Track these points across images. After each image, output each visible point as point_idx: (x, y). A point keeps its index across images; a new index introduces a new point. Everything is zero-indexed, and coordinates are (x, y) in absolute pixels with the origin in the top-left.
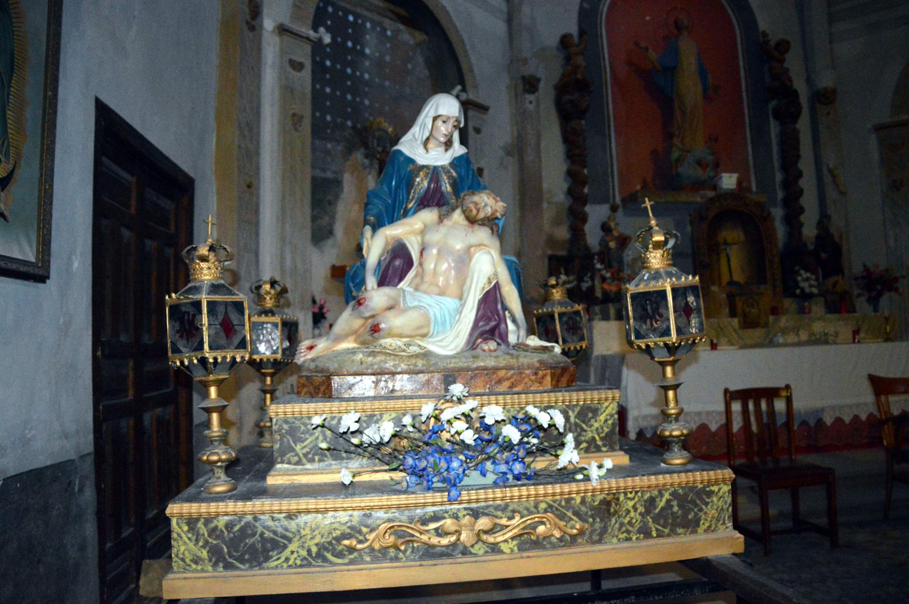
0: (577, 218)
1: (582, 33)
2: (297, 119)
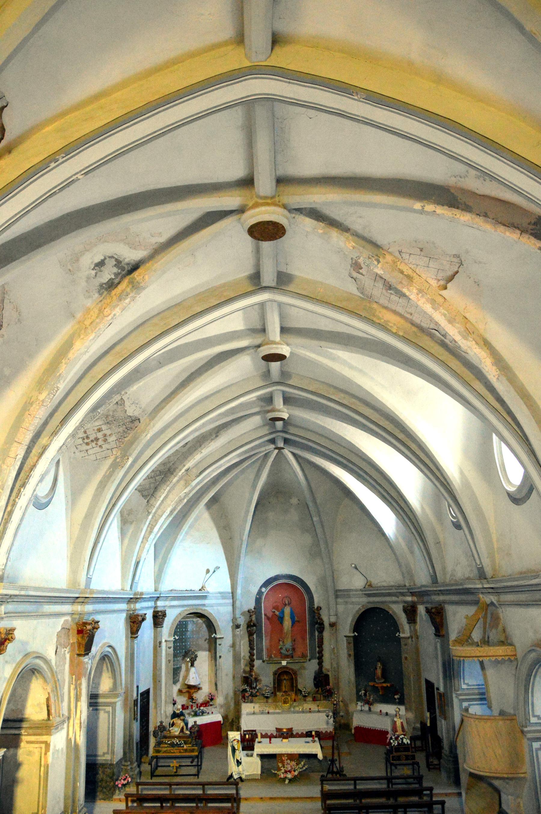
0: (252, 666)
2: (169, 661)
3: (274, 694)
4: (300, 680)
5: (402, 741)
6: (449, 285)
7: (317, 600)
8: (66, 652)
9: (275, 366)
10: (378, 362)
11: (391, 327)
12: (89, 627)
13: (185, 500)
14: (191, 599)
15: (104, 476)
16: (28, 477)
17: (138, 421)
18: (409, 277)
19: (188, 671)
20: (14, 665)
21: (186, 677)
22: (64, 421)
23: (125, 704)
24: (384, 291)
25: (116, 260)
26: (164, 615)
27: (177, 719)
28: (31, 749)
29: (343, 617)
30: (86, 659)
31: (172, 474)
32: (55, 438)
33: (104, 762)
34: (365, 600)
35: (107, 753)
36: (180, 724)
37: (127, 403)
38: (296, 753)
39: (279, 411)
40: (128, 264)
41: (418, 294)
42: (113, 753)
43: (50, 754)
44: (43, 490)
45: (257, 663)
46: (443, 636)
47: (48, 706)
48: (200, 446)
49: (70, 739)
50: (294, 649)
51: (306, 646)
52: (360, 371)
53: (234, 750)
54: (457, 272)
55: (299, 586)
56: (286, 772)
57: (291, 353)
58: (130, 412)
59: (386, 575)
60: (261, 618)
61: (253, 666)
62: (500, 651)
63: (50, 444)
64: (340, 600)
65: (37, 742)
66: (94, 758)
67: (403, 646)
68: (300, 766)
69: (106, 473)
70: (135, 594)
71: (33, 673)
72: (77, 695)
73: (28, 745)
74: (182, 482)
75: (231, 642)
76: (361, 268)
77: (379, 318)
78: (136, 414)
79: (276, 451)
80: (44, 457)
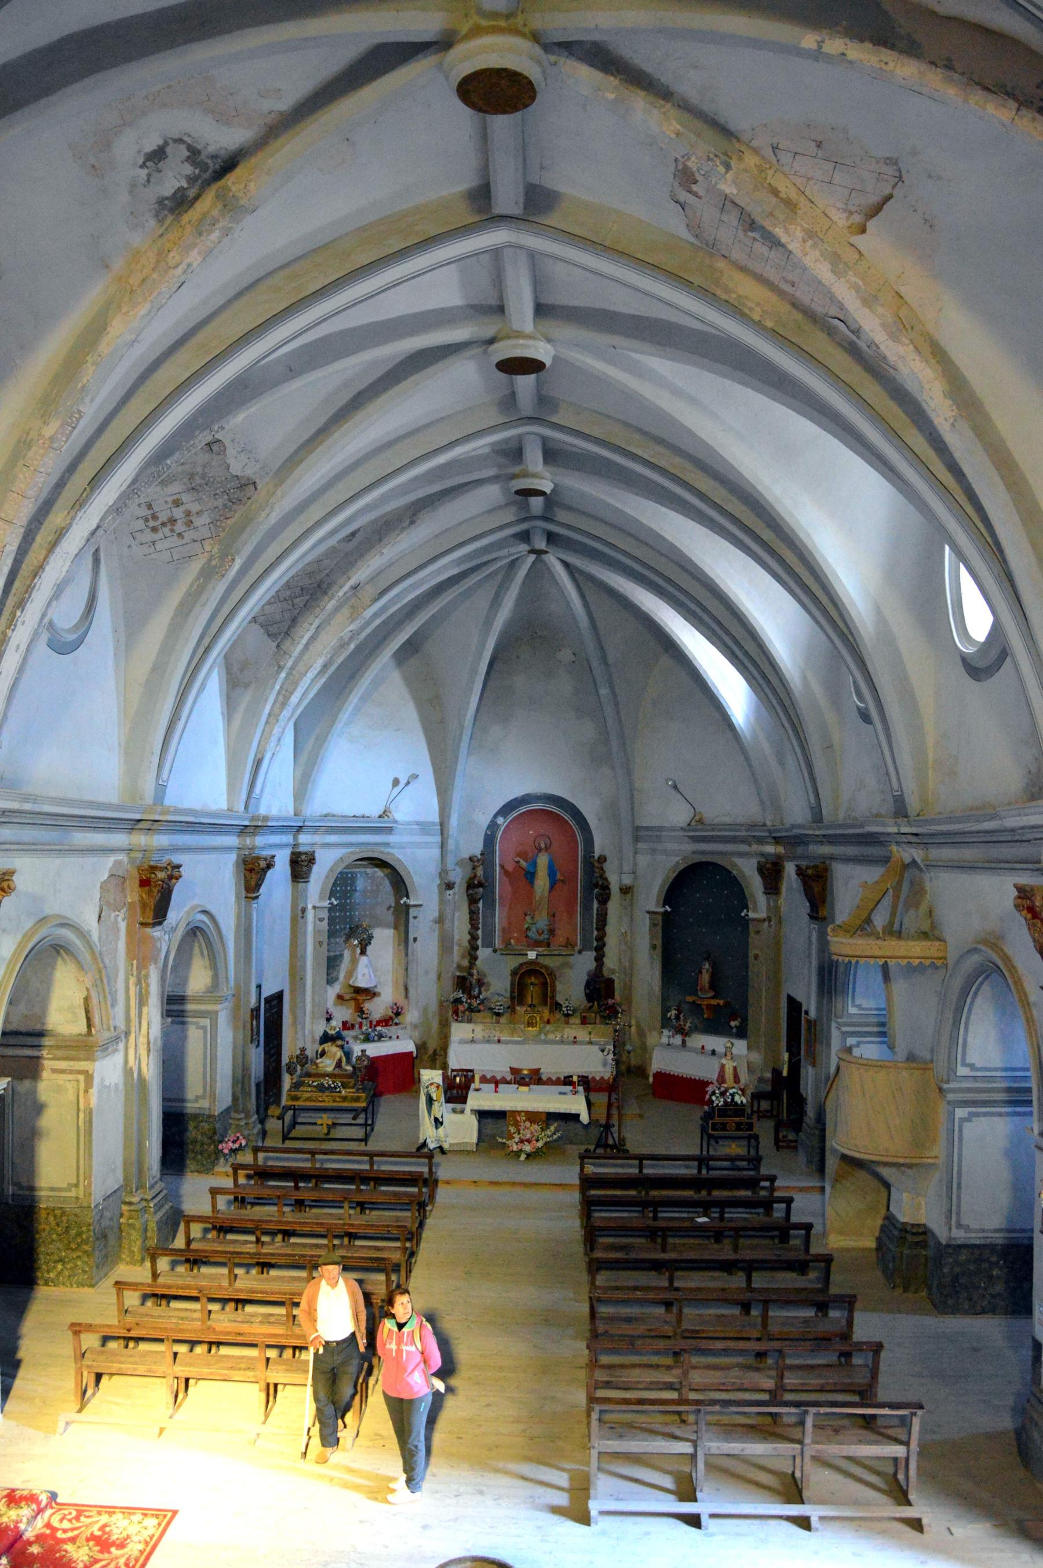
0: (473, 958)
1: (482, 854)
2: (321, 943)
3: (511, 1009)
4: (559, 987)
5: (733, 1099)
6: (871, 225)
7: (601, 844)
8: (120, 919)
9: (525, 383)
10: (728, 382)
11: (751, 309)
12: (161, 875)
13: (352, 646)
14: (365, 833)
15: (188, 594)
16: (29, 589)
17: (252, 487)
18: (790, 205)
19: (354, 962)
20: (19, 937)
21: (350, 973)
22: (96, 482)
23: (235, 1016)
24: (741, 234)
25: (190, 148)
26: (311, 860)
27: (329, 1044)
28: (60, 1082)
29: (644, 877)
30: (156, 932)
31: (325, 593)
32: (80, 514)
33: (198, 1111)
34: (689, 847)
35: (203, 1097)
36: (335, 1054)
37: (231, 452)
38: (541, 1110)
39: (534, 476)
40: (214, 157)
41: (804, 241)
42: (213, 1097)
43: (94, 1091)
44: (67, 613)
45: (483, 953)
46: (824, 919)
47: (87, 1011)
48: (380, 540)
49: (131, 1069)
50: (552, 932)
51: (573, 926)
52: (693, 400)
53: (430, 1101)
54: (889, 197)
55: (567, 817)
56: (522, 1141)
57: (555, 358)
58: (236, 469)
59: (730, 804)
60: (494, 871)
61: (476, 958)
62: (916, 949)
63: (70, 525)
64: (640, 845)
65: (71, 1072)
66: (180, 1104)
67: (752, 934)
68: (549, 1133)
69: (191, 586)
70: (253, 819)
71: (58, 953)
72: (140, 993)
73: (55, 1076)
74: (346, 611)
75: (436, 914)
76: (695, 182)
77: (728, 291)
78: (249, 472)
79: (532, 557)
80: (58, 550)
